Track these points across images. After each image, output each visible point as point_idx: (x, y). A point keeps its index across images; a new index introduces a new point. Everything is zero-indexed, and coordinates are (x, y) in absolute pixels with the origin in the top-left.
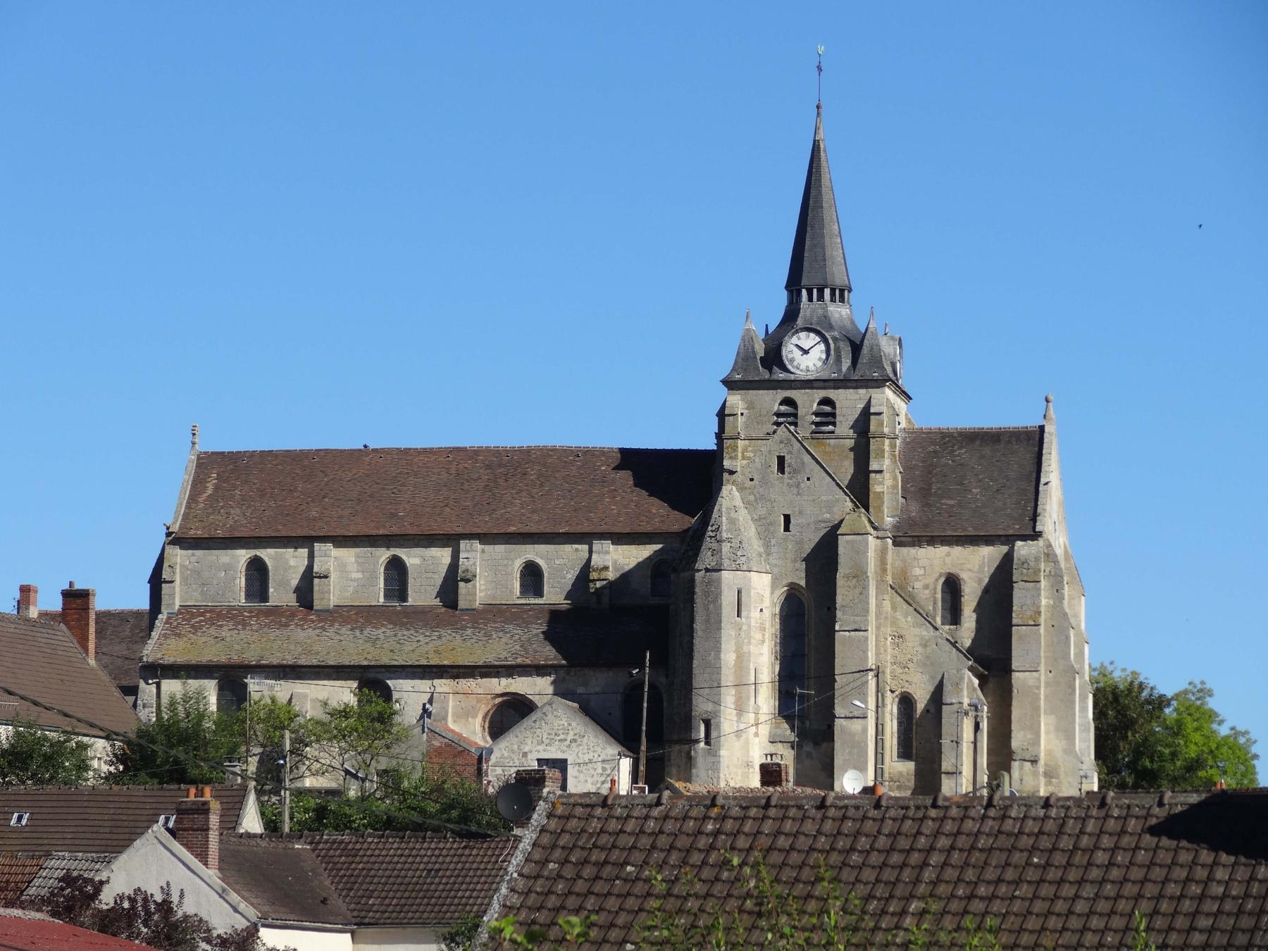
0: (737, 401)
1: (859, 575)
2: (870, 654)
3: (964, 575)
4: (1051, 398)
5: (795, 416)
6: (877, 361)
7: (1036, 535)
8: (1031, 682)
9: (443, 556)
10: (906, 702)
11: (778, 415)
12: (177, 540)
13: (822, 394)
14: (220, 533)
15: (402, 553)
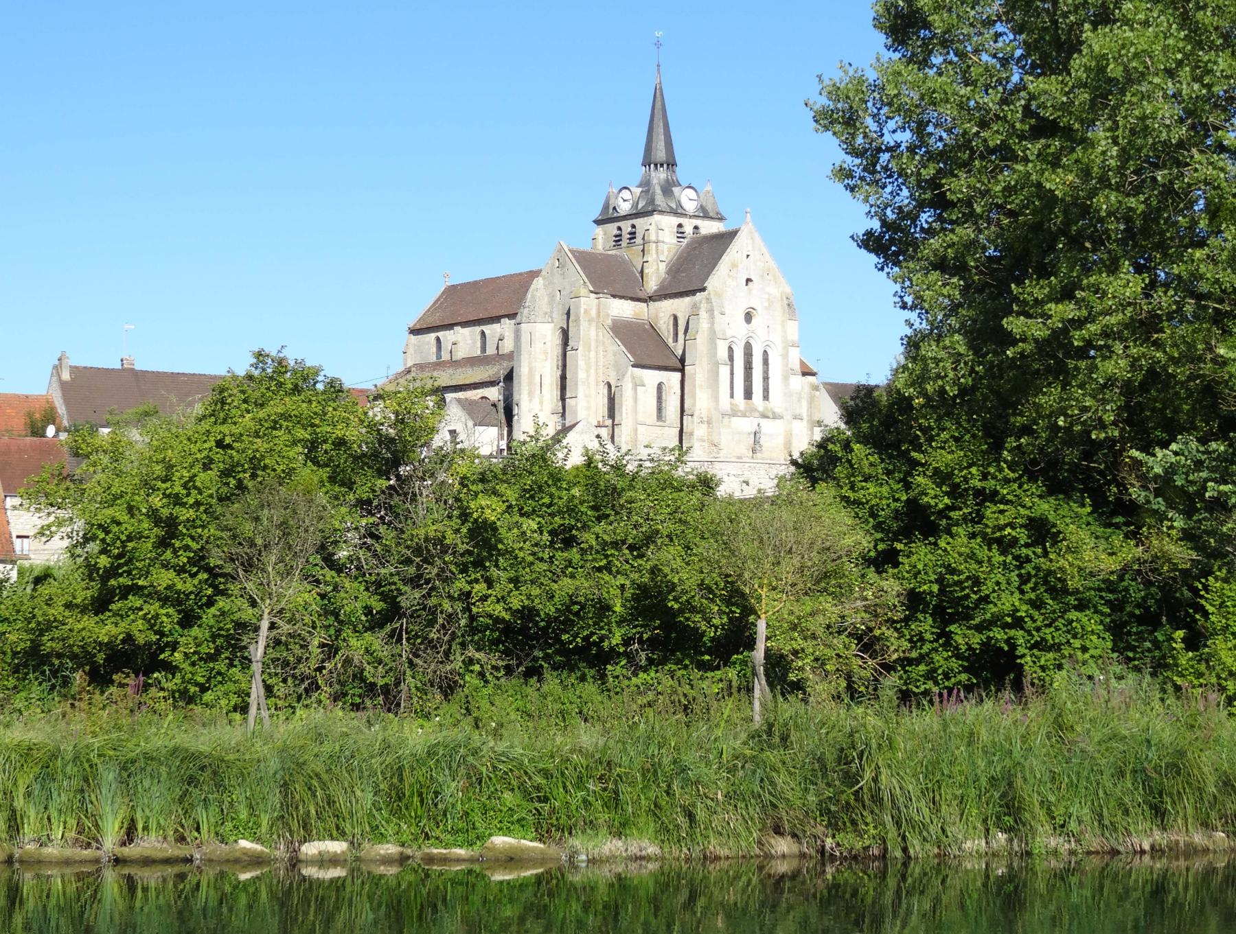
0: (599, 231)
1: (577, 320)
2: (581, 363)
3: (680, 315)
4: (748, 210)
5: (620, 235)
6: (652, 201)
7: (704, 289)
8: (693, 372)
9: (496, 326)
10: (609, 386)
11: (616, 236)
12: (414, 331)
13: (630, 222)
14: (425, 326)
15: (484, 328)
